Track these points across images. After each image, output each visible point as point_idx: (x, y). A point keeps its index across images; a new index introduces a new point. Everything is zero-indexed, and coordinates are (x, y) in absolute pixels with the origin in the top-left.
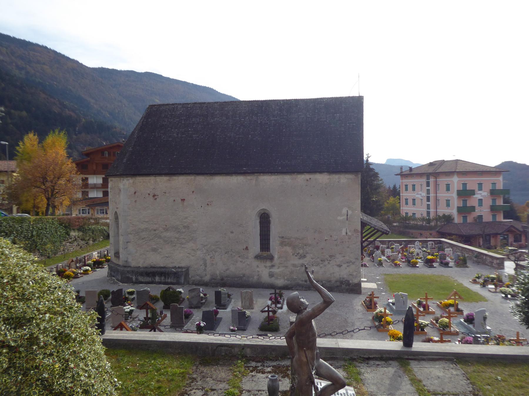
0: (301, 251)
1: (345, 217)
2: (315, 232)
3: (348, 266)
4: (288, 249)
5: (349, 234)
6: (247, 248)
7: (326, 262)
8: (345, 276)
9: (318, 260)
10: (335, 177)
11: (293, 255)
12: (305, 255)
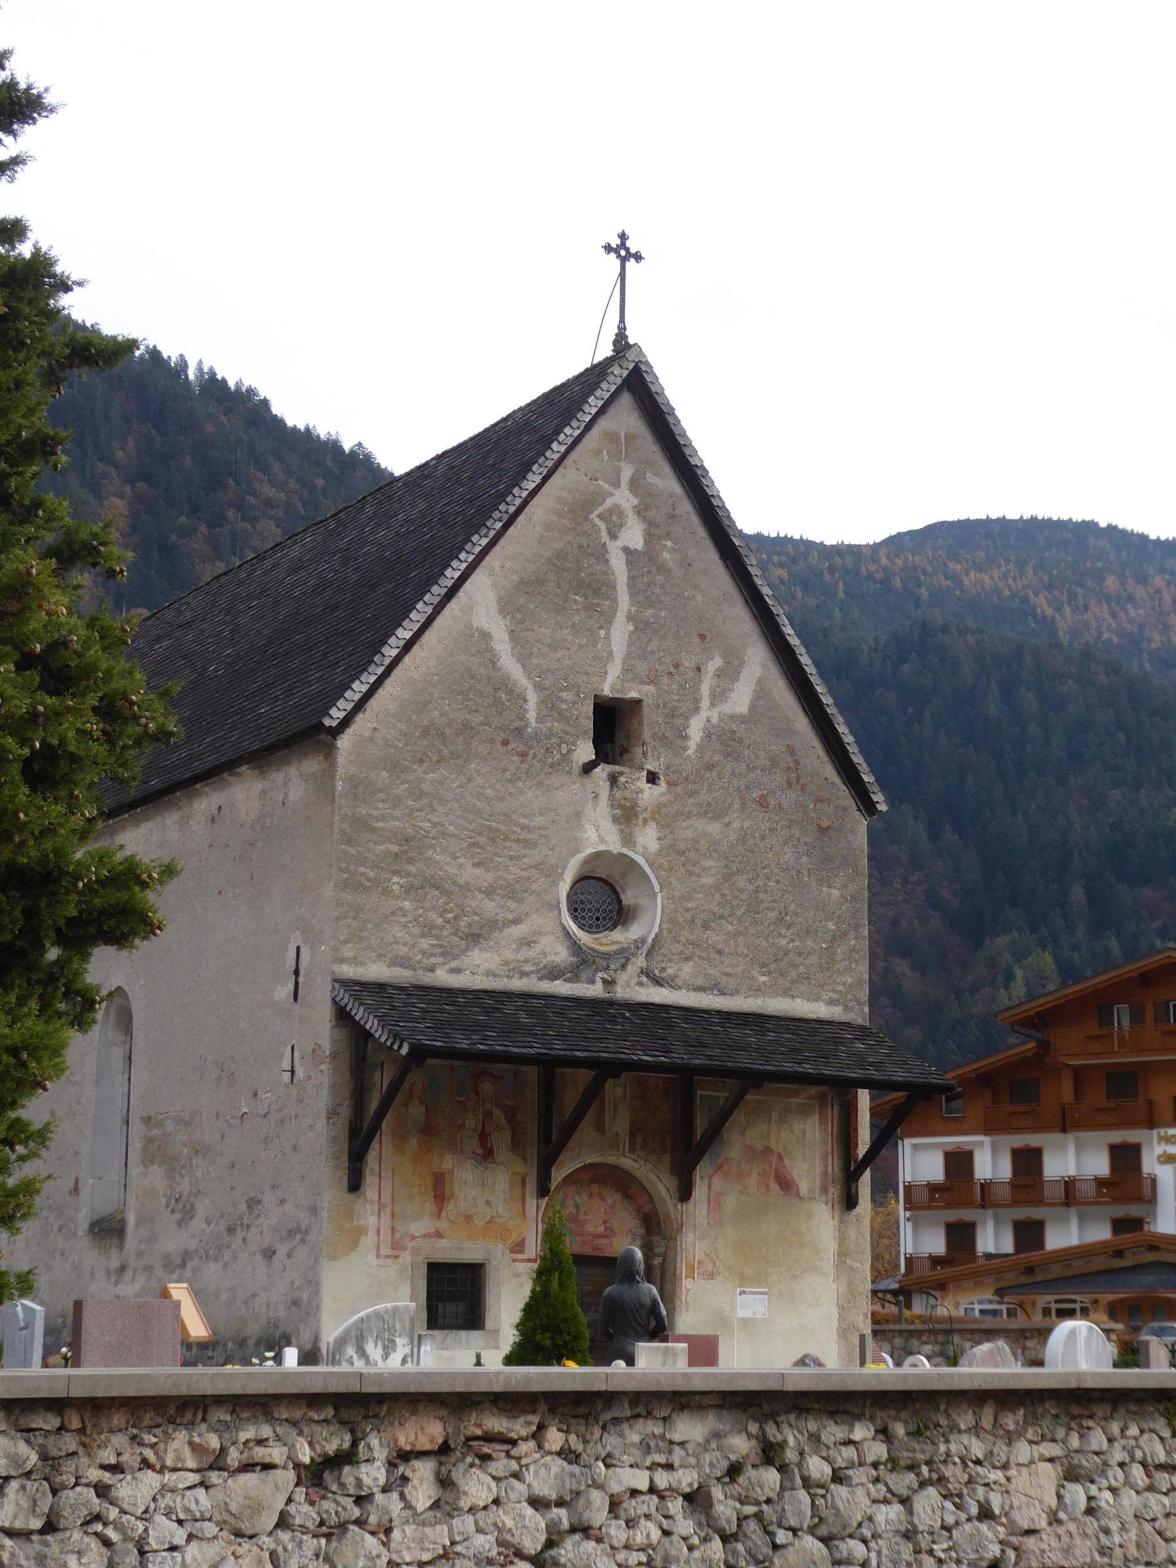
0: (185, 1186)
1: (291, 986)
2: (219, 1078)
3: (289, 1256)
4: (157, 1174)
5: (300, 1073)
6: (76, 1190)
7: (240, 1235)
8: (281, 1313)
9: (222, 1227)
10: (278, 777)
11: (167, 1206)
12: (193, 1209)
